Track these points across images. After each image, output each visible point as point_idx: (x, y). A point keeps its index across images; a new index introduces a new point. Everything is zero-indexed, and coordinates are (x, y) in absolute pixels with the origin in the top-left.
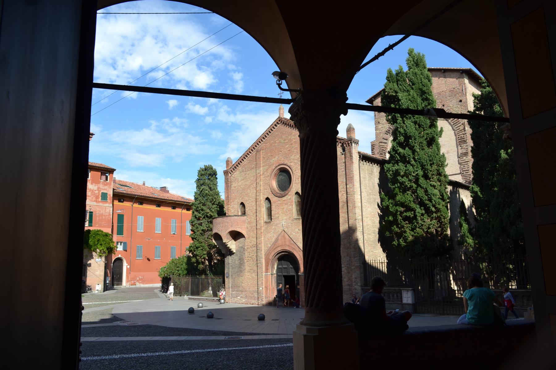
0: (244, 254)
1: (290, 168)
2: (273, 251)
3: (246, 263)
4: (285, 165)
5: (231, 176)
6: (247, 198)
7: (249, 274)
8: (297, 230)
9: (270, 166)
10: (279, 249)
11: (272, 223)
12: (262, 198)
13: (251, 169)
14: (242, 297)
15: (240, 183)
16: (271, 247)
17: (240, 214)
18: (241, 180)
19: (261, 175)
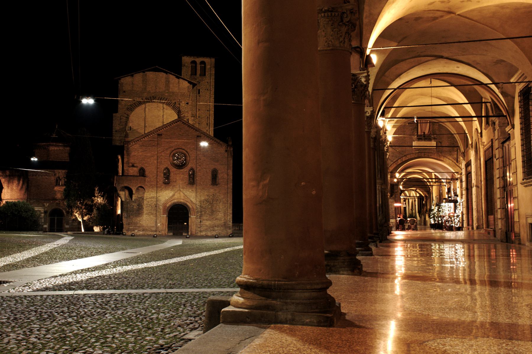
0: (143, 202)
1: (186, 151)
2: (170, 202)
3: (145, 209)
4: (184, 149)
5: (131, 146)
6: (146, 165)
7: (147, 216)
8: (191, 190)
9: (170, 148)
10: (176, 201)
11: (170, 184)
12: (162, 167)
13: (151, 146)
14: (139, 231)
15: (140, 154)
16: (168, 199)
17: (138, 175)
18: (142, 152)
19: (161, 152)
